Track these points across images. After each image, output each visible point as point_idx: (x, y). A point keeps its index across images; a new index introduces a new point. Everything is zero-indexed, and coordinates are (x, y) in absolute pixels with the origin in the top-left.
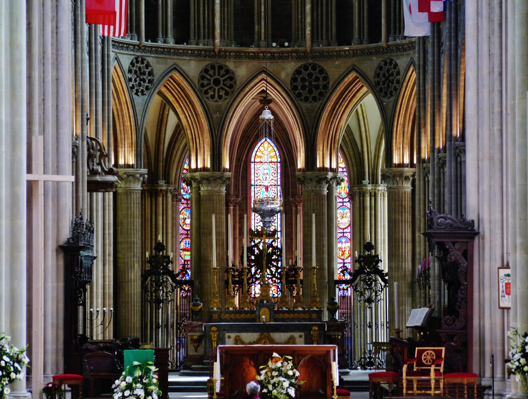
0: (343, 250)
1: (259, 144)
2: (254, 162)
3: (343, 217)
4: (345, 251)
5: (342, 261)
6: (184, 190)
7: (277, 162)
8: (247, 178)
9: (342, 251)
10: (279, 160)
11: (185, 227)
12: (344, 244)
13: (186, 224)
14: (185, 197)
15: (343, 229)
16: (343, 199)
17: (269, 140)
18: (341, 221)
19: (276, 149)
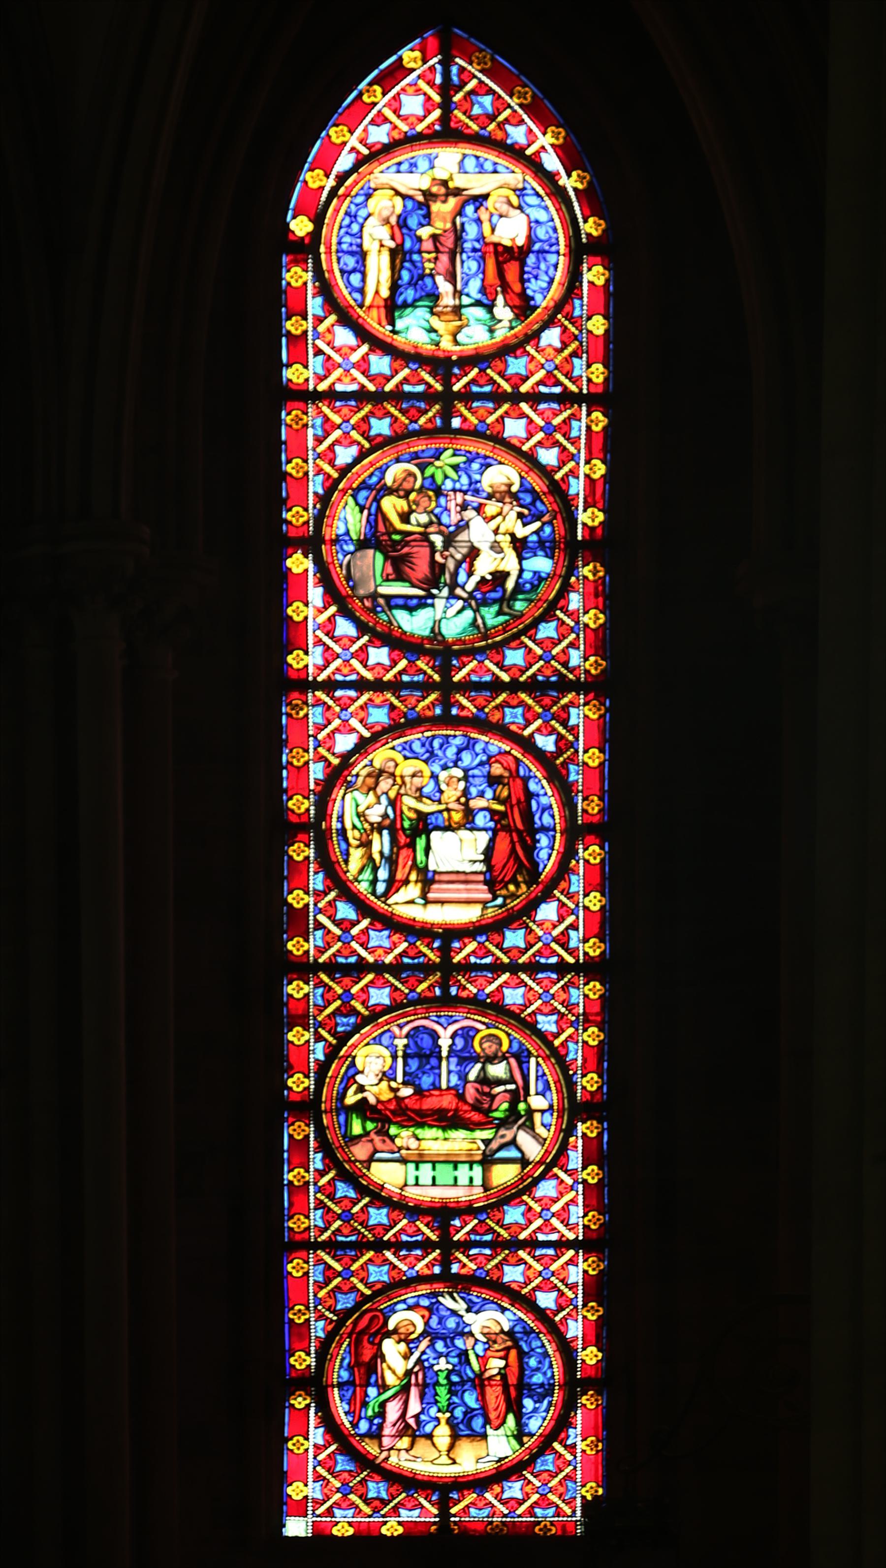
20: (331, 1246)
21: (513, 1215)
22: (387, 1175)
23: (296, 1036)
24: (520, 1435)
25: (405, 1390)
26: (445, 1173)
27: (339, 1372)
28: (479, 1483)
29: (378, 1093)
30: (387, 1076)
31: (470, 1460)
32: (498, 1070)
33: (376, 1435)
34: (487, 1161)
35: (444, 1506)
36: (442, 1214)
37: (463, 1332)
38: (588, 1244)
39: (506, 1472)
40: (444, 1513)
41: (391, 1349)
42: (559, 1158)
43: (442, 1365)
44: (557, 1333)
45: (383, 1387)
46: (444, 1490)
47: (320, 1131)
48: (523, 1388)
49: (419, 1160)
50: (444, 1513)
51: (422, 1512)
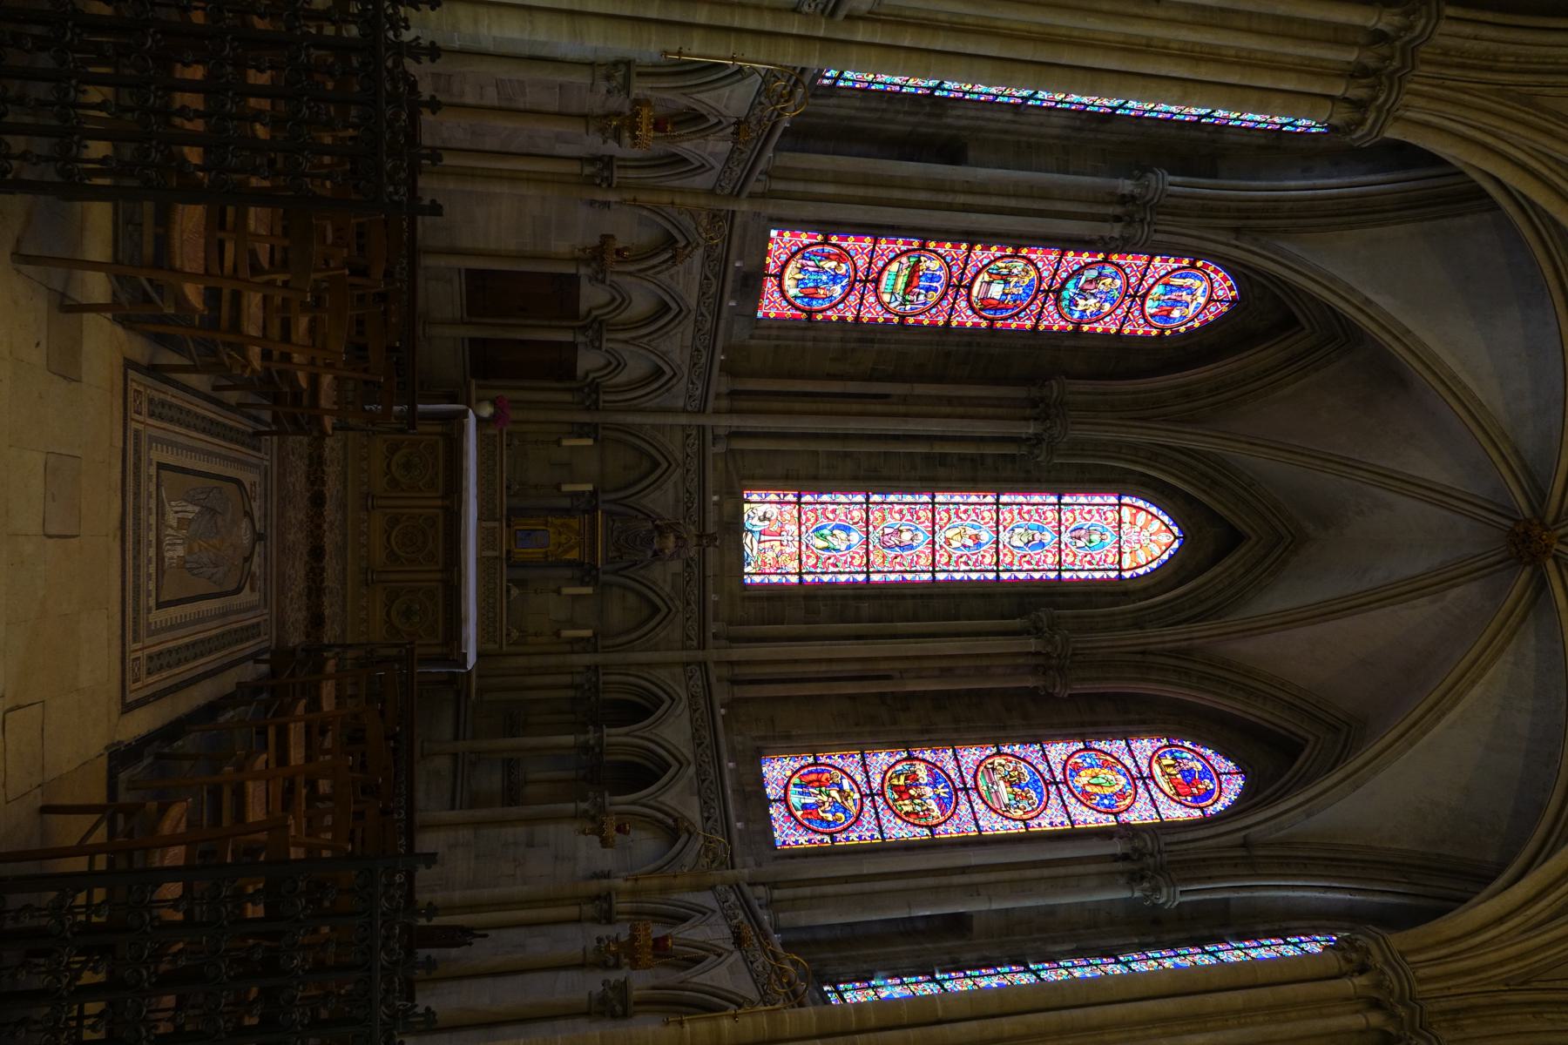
0: (912, 792)
1: (1166, 519)
2: (1121, 505)
4: (912, 798)
5: (876, 785)
6: (1089, 281)
7: (1121, 570)
8: (1082, 481)
9: (908, 787)
10: (1127, 575)
11: (985, 277)
12: (928, 791)
13: (989, 283)
14: (1070, 285)
15: (976, 788)
16: (1065, 782)
17: (1176, 545)
18: (996, 777)
19: (1154, 565)
20: (873, 250)
21: (872, 299)
22: (894, 267)
23: (948, 245)
24: (796, 297)
27: (827, 249)
28: (780, 285)
29: (923, 266)
31: (789, 283)
32: (922, 297)
33: (804, 258)
35: (775, 276)
36: (877, 281)
37: (835, 283)
38: (857, 318)
42: (887, 311)
43: (824, 278)
44: (830, 308)
46: (780, 276)
49: (897, 276)
51: (772, 269)
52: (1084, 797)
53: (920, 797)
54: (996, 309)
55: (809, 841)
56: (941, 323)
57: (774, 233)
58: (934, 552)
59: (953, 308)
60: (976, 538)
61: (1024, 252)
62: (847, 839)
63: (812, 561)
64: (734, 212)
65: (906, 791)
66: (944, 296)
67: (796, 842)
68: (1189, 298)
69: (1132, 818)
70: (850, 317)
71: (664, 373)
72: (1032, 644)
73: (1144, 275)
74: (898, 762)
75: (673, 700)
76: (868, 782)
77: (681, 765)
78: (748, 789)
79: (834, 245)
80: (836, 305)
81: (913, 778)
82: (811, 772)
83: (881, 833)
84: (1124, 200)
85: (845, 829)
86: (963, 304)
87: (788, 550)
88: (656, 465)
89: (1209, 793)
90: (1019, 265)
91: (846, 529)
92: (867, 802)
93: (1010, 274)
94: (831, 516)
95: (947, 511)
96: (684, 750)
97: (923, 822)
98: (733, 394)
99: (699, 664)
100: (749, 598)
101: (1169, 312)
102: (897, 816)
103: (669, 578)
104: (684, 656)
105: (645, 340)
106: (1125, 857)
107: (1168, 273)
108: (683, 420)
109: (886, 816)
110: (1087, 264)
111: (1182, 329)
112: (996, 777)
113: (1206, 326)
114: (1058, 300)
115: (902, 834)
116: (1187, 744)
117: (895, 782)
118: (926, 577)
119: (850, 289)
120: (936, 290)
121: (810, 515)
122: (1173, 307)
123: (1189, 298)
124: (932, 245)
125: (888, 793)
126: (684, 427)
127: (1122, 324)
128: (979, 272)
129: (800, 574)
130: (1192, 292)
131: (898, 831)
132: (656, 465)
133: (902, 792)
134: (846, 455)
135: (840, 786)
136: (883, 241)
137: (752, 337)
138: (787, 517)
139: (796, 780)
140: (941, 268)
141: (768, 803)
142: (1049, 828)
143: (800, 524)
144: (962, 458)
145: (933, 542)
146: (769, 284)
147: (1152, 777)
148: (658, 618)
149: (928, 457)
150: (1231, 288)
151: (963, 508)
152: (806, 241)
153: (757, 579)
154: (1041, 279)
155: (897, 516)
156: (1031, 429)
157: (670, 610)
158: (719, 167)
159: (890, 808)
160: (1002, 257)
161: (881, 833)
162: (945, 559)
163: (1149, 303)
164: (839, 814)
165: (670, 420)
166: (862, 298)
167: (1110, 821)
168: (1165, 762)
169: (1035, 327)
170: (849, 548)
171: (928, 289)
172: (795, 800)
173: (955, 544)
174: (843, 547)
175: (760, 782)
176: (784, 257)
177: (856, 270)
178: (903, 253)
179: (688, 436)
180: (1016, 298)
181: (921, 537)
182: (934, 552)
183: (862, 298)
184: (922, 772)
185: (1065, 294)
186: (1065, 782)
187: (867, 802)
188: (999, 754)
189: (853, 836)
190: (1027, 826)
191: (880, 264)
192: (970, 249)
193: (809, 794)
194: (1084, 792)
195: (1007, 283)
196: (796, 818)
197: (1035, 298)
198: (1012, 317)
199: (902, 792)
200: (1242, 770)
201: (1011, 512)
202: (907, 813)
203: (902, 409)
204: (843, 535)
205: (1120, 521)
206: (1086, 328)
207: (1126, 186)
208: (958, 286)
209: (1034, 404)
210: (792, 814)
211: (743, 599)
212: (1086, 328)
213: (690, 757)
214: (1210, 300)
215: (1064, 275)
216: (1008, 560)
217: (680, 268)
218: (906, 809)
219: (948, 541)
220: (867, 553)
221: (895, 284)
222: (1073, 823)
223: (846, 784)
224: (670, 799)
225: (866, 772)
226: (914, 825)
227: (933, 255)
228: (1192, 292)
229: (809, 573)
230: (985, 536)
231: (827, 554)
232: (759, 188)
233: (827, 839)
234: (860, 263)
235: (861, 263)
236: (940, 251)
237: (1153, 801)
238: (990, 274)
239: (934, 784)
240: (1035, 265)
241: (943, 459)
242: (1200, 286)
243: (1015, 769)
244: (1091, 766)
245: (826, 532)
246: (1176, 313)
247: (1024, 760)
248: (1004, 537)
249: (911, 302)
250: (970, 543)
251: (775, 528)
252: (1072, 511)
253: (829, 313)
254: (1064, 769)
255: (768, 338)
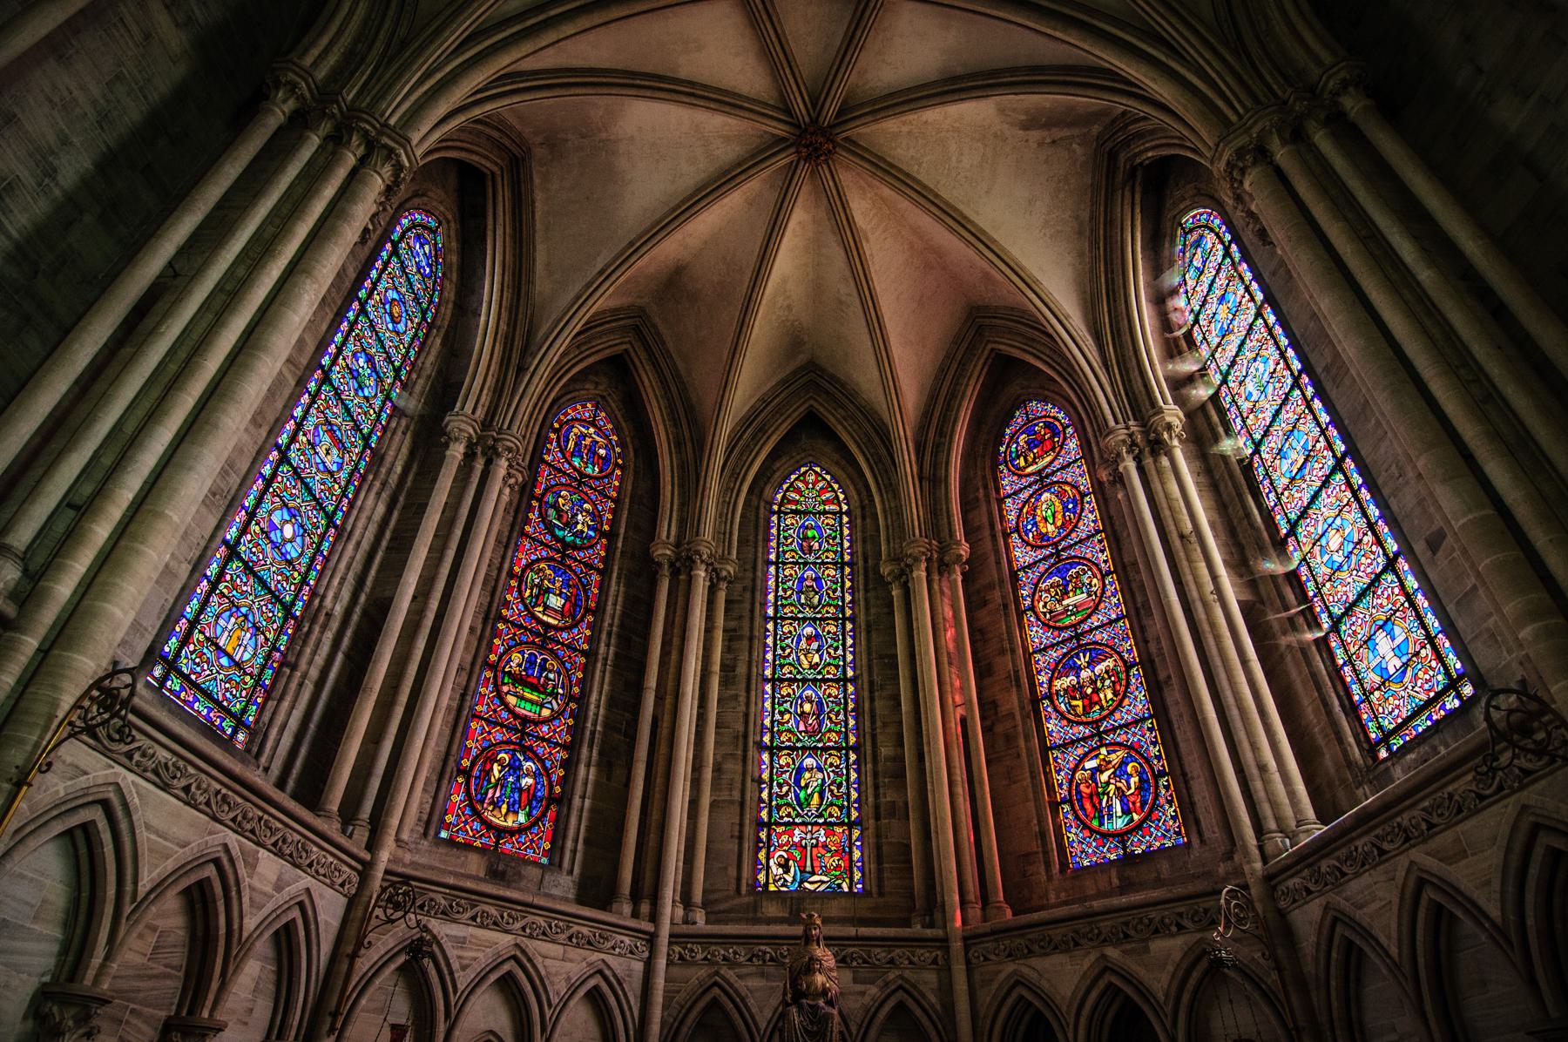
0: (1089, 691)
3: (1065, 594)
7: (840, 512)
9: (1084, 696)
12: (1084, 674)
13: (546, 607)
14: (560, 533)
15: (1075, 626)
20: (486, 720)
21: (545, 728)
22: (512, 700)
23: (497, 641)
24: (529, 815)
25: (495, 787)
26: (528, 706)
27: (476, 772)
28: (512, 832)
30: (519, 665)
32: (551, 676)
33: (482, 802)
34: (542, 706)
35: (498, 838)
36: (525, 720)
37: (520, 767)
39: (521, 830)
40: (497, 843)
41: (496, 767)
42: (562, 713)
44: (549, 777)
45: (489, 782)
46: (501, 832)
47: (495, 677)
48: (535, 796)
49: (522, 698)
50: (497, 843)
51: (490, 840)
52: (1069, 526)
53: (1093, 682)
54: (576, 605)
55: (1170, 803)
56: (583, 660)
57: (444, 834)
58: (824, 680)
59: (568, 646)
60: (810, 639)
61: (517, 569)
62: (1159, 758)
63: (835, 811)
64: (387, 872)
65: (1089, 697)
66: (553, 653)
67: (1174, 818)
68: (588, 441)
69: (1085, 483)
70: (563, 755)
71: (596, 988)
72: (920, 573)
73: (559, 470)
74: (1056, 709)
75: (1017, 983)
76: (1085, 739)
77: (1106, 969)
78: (1116, 881)
79: (473, 764)
80: (546, 770)
81: (1074, 691)
82: (1082, 808)
83: (1144, 719)
84: (469, 456)
85: (1147, 761)
86: (565, 635)
87: (822, 839)
88: (715, 1002)
89: (1048, 426)
90: (531, 575)
91: (800, 771)
92: (1109, 738)
93: (539, 586)
94: (785, 789)
95: (782, 666)
96: (1087, 963)
97: (1123, 676)
98: (635, 898)
99: (967, 948)
100: (880, 886)
101: (600, 457)
102: (1120, 704)
103: (859, 987)
104: (959, 971)
105: (548, 1013)
106: (1138, 460)
107: (561, 451)
108: (662, 963)
109: (1121, 717)
110: (541, 515)
111: (618, 450)
112: (1059, 608)
113: (617, 430)
114: (574, 547)
115: (1141, 696)
116: (1002, 449)
117: (1080, 710)
118: (851, 688)
119: (531, 754)
120: (545, 660)
121: (783, 812)
122: (595, 453)
123: (588, 441)
124: (493, 658)
125: (1095, 714)
126: (670, 963)
127: (606, 496)
128: (534, 617)
129: (851, 825)
130: (584, 436)
131: (1138, 703)
132: (715, 1002)
133: (1090, 702)
134: (718, 769)
135: (1095, 771)
136: (479, 708)
137: (571, 872)
138: (785, 838)
139: (1095, 823)
140: (522, 653)
141: (1129, 859)
142: (1107, 552)
143: (794, 824)
144: (728, 649)
145: (814, 681)
146: (508, 846)
147: (1039, 472)
148: (910, 1003)
149: (725, 682)
150: (584, 406)
151: (779, 652)
152: (462, 796)
153: (857, 875)
154: (548, 559)
155: (787, 717)
156: (701, 573)
157: (900, 987)
158: (307, 881)
159: (1112, 713)
160: (520, 591)
161: (1144, 719)
162: (832, 670)
163: (589, 471)
164: (1129, 769)
165: (660, 982)
166: (543, 739)
167: (1091, 501)
168: (1022, 463)
169: (600, 572)
170: (820, 769)
171: (543, 668)
172: (1120, 824)
173: (816, 659)
174: (820, 775)
175: (1103, 867)
176: (476, 825)
177: (509, 742)
178: (497, 688)
179: (681, 957)
180: (566, 584)
181: (809, 692)
182: (824, 680)
183: (543, 739)
184: (1062, 683)
185: (569, 539)
186: (1055, 545)
187: (1109, 738)
188: (1032, 608)
189: (1154, 751)
190: (1109, 573)
191: (505, 714)
192: (505, 620)
193: (1110, 807)
194: (1063, 526)
195: (548, 591)
196: (1142, 822)
197: (570, 567)
198: (586, 592)
199: (1090, 702)
200: (1020, 403)
201: (784, 606)
202: (1115, 693)
203: (669, 700)
204: (807, 775)
205: (796, 512)
206: (606, 527)
207: (457, 451)
208: (544, 638)
209: (675, 573)
210: (1139, 826)
211: (881, 894)
212: (606, 527)
213: (1092, 957)
214: (593, 424)
215: (549, 537)
216: (832, 610)
217: (452, 953)
218: (1110, 696)
219: (813, 666)
220: (825, 749)
221: (532, 702)
222: (1098, 532)
223: (1091, 764)
224: (1159, 983)
225: (1072, 742)
226: (1128, 685)
227: (505, 658)
228: (584, 436)
229: (849, 815)
230: (809, 630)
231: (828, 794)
232: (361, 835)
233: (1163, 781)
234: (499, 737)
235: (498, 735)
236: (501, 649)
237: (1063, 468)
238: (536, 605)
239: (1077, 670)
240: (534, 562)
241: (728, 668)
242: (578, 429)
243: (1047, 591)
244: (1035, 525)
245: (802, 795)
246: (602, 452)
247: (1036, 585)
248: (808, 613)
249: (555, 687)
250: (815, 645)
251: (797, 854)
252: (785, 552)
253: (554, 778)
254: (1041, 547)
255: (574, 851)
